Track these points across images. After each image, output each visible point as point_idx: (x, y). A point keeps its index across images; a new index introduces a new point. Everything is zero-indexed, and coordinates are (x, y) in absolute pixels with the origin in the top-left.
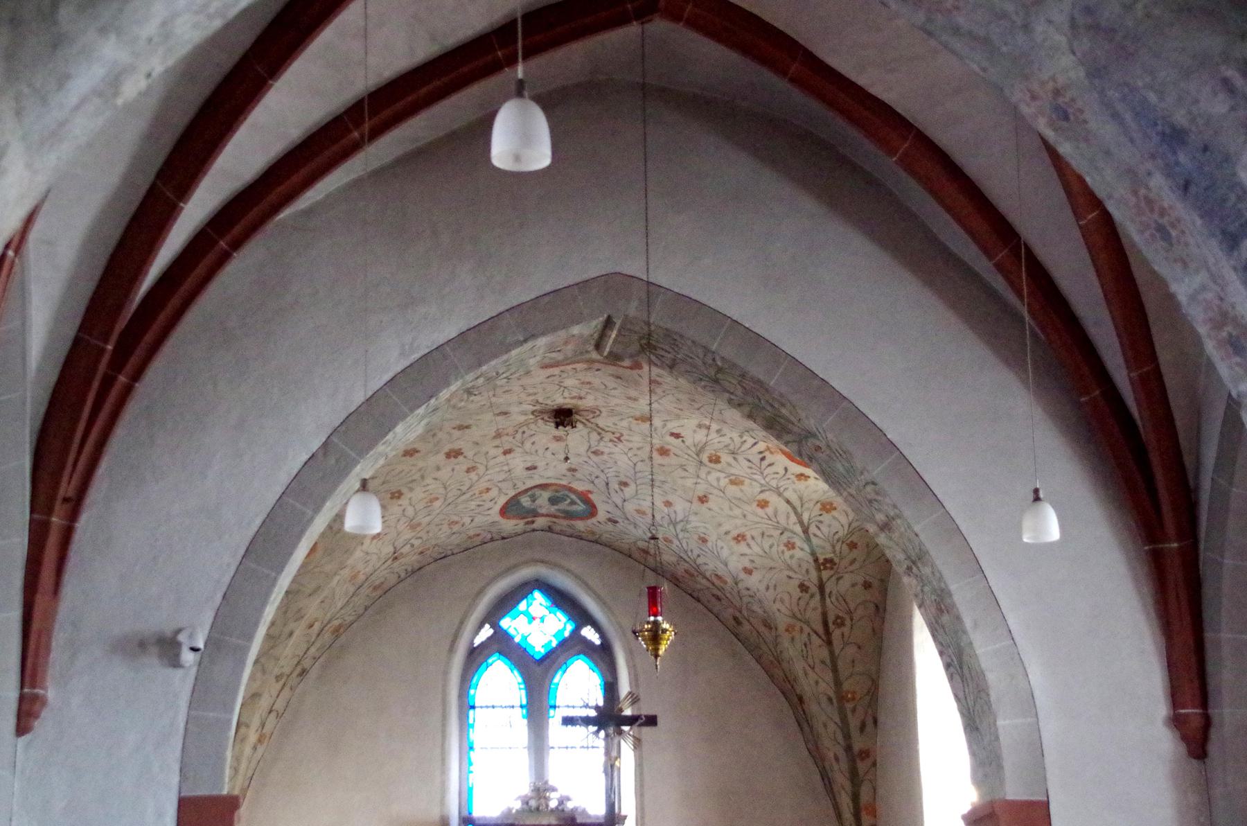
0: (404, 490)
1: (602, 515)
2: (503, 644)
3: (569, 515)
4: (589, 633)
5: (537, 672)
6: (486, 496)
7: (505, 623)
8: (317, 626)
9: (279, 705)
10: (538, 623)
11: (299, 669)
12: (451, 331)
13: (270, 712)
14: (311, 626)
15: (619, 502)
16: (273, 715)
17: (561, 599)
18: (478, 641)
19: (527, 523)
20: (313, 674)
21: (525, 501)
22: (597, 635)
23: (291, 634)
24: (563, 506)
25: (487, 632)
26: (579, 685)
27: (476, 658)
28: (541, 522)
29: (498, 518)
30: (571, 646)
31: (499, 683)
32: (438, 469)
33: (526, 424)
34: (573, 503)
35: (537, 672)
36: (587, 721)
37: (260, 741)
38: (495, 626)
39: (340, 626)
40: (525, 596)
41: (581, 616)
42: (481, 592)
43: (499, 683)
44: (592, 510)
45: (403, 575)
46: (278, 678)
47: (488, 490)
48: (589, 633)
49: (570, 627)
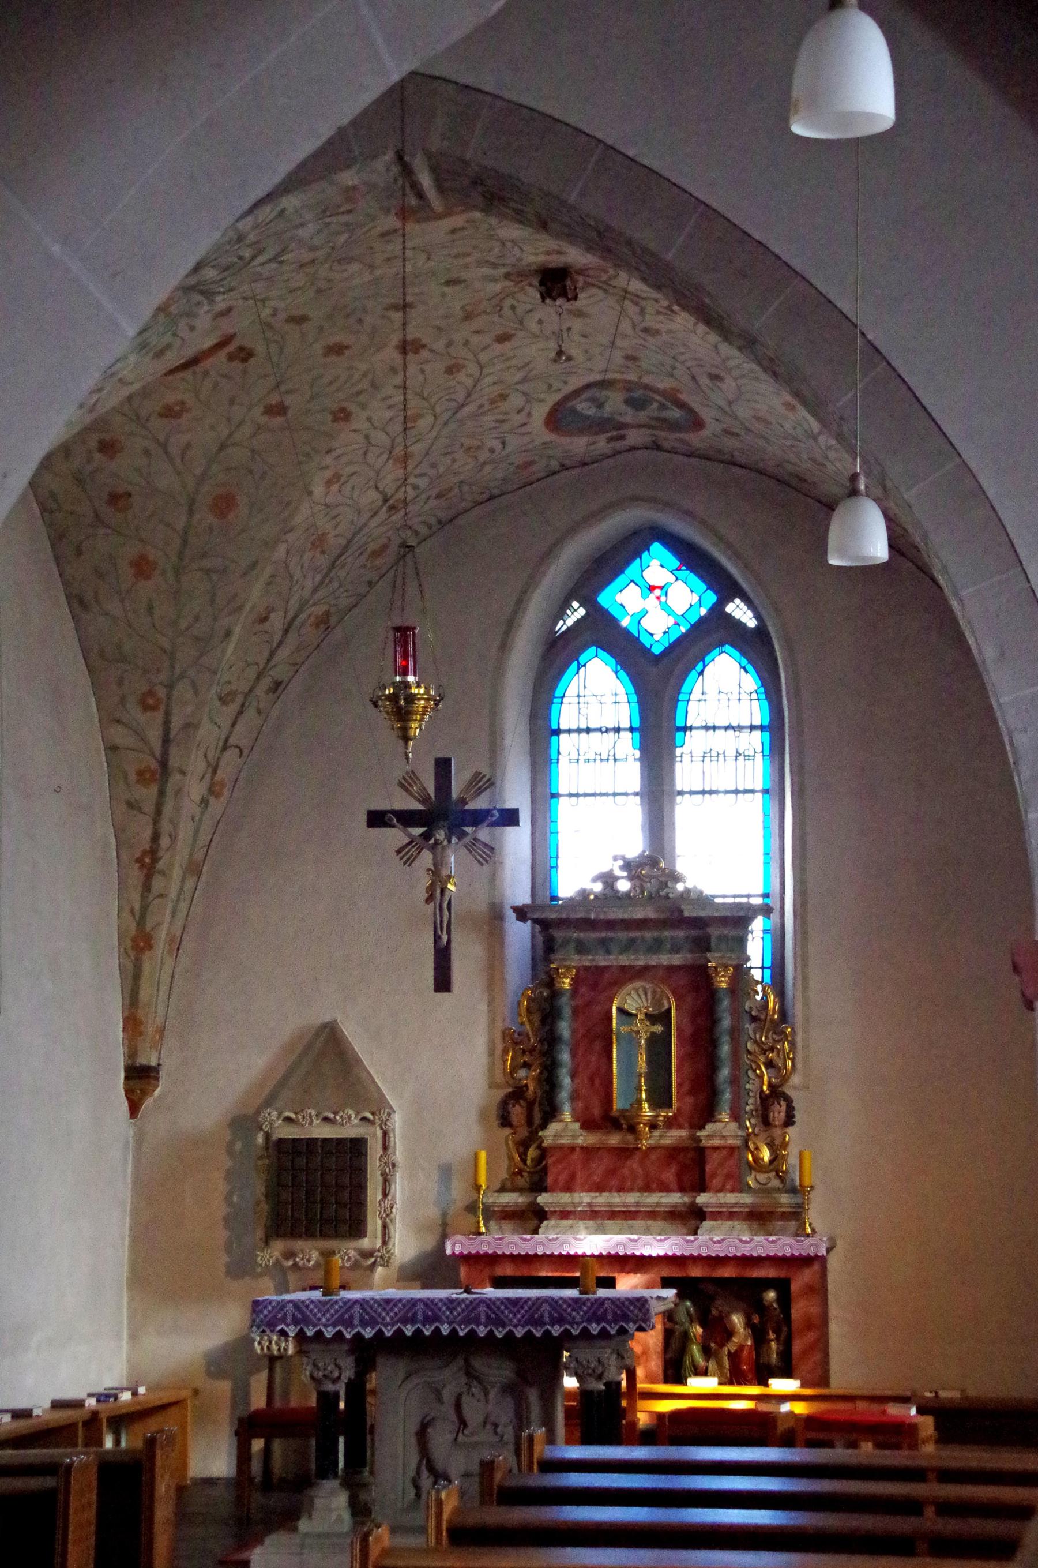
0: (352, 408)
1: (711, 428)
4: (739, 611)
5: (658, 678)
6: (504, 406)
7: (604, 599)
8: (277, 620)
9: (241, 736)
11: (266, 682)
13: (225, 748)
14: (264, 619)
15: (723, 404)
16: (231, 754)
17: (692, 558)
18: (561, 626)
19: (611, 439)
20: (295, 688)
22: (750, 614)
23: (228, 634)
25: (577, 613)
28: (633, 437)
29: (549, 437)
31: (596, 692)
33: (504, 295)
34: (662, 407)
35: (658, 678)
36: (406, 818)
37: (213, 791)
39: (328, 614)
40: (637, 554)
43: (596, 692)
46: (224, 700)
47: (503, 397)
49: (711, 598)
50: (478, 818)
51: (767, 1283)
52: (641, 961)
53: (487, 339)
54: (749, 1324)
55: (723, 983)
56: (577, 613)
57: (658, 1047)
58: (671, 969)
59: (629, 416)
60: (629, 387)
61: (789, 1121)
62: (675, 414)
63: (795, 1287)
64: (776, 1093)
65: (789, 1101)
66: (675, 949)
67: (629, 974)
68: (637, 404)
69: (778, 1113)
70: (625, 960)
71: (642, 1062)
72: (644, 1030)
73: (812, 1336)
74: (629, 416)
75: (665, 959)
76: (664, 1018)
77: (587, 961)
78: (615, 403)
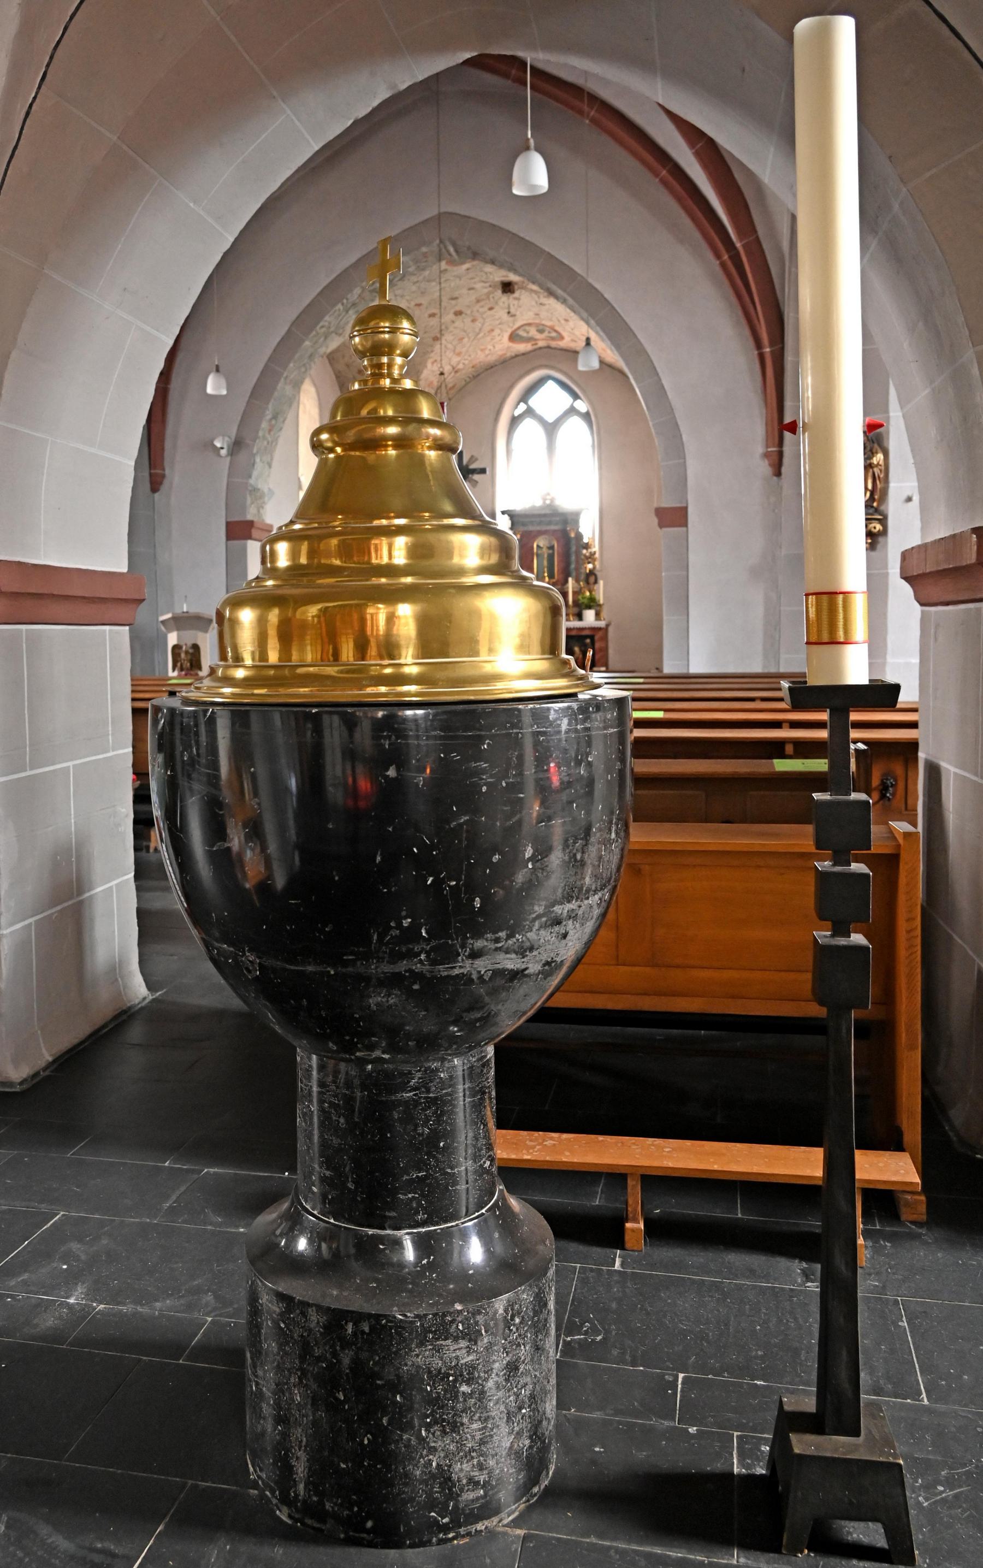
2: (530, 412)
3: (553, 339)
5: (551, 429)
10: (551, 399)
12: (353, 259)
18: (517, 413)
21: (521, 333)
24: (546, 334)
25: (522, 407)
26: (577, 435)
27: (515, 421)
28: (541, 344)
30: (572, 411)
32: (453, 322)
35: (551, 429)
38: (526, 403)
41: (576, 396)
42: (511, 387)
44: (562, 338)
45: (468, 380)
47: (492, 330)
48: (582, 406)
50: (474, 471)
51: (587, 637)
52: (544, 528)
53: (486, 309)
54: (581, 650)
55: (573, 535)
56: (522, 407)
57: (551, 558)
58: (555, 531)
59: (538, 336)
60: (537, 325)
61: (596, 582)
62: (554, 334)
63: (596, 638)
64: (592, 572)
65: (596, 576)
66: (556, 524)
67: (540, 533)
68: (541, 331)
69: (592, 579)
70: (538, 528)
71: (545, 563)
72: (545, 552)
73: (601, 654)
74: (538, 336)
75: (553, 527)
76: (552, 548)
77: (526, 529)
78: (533, 332)
